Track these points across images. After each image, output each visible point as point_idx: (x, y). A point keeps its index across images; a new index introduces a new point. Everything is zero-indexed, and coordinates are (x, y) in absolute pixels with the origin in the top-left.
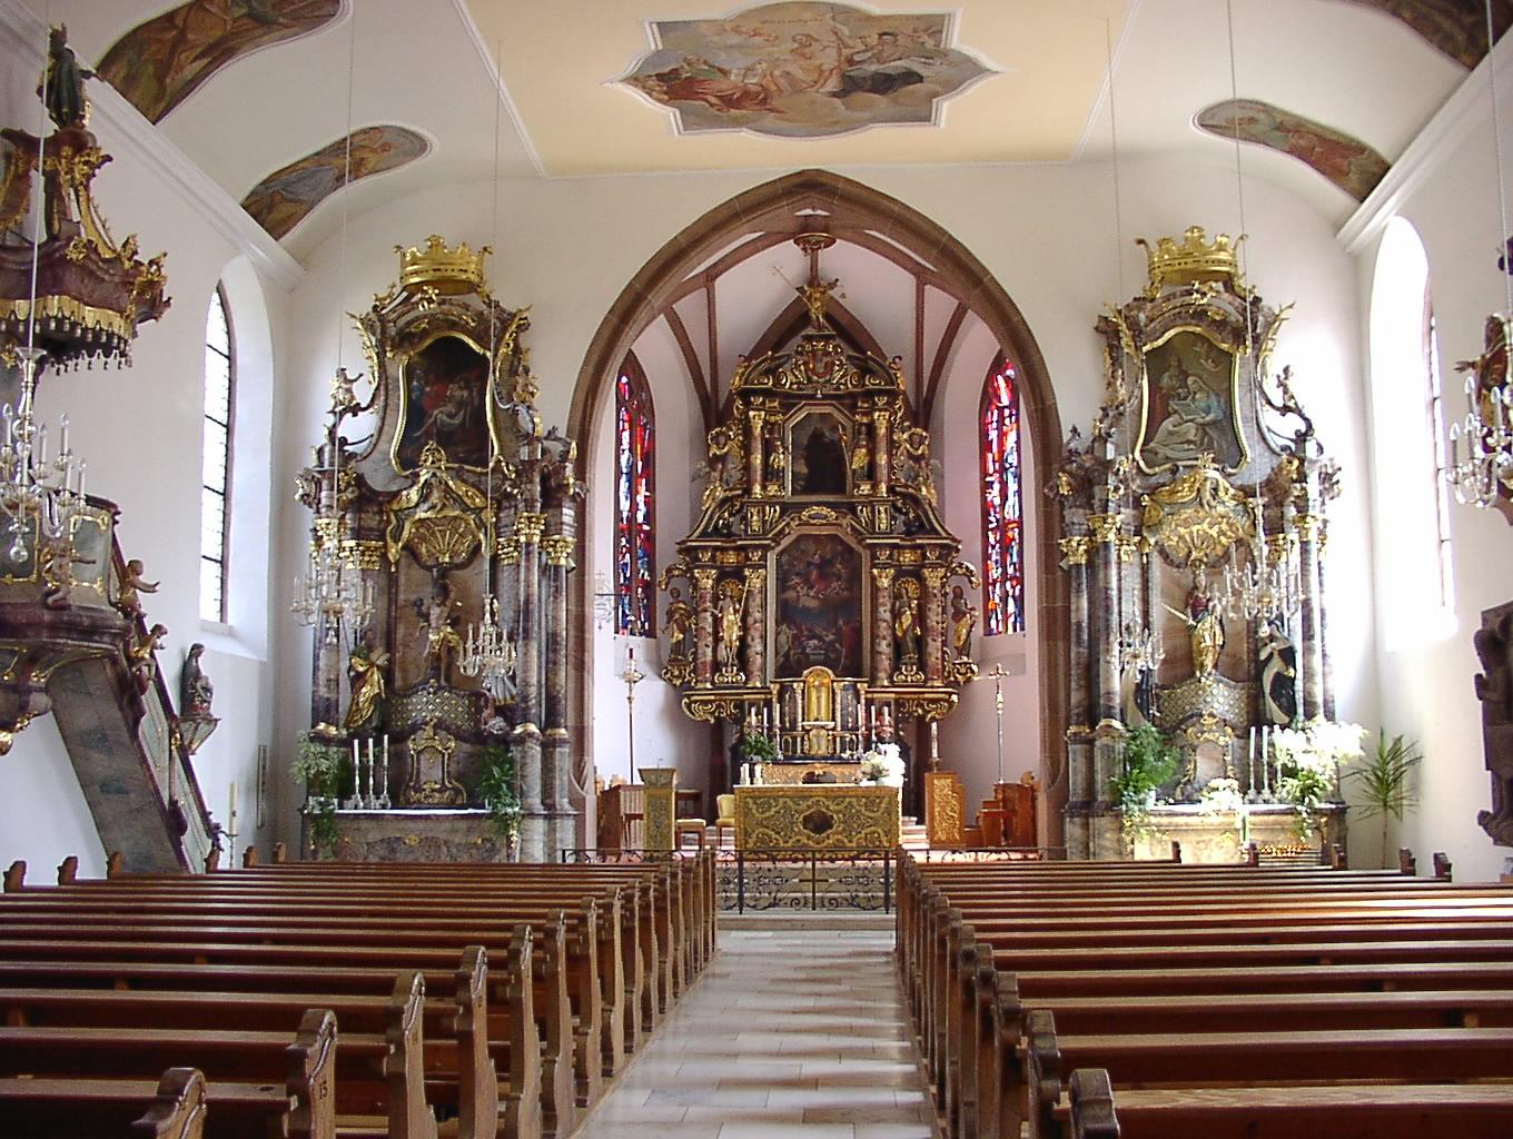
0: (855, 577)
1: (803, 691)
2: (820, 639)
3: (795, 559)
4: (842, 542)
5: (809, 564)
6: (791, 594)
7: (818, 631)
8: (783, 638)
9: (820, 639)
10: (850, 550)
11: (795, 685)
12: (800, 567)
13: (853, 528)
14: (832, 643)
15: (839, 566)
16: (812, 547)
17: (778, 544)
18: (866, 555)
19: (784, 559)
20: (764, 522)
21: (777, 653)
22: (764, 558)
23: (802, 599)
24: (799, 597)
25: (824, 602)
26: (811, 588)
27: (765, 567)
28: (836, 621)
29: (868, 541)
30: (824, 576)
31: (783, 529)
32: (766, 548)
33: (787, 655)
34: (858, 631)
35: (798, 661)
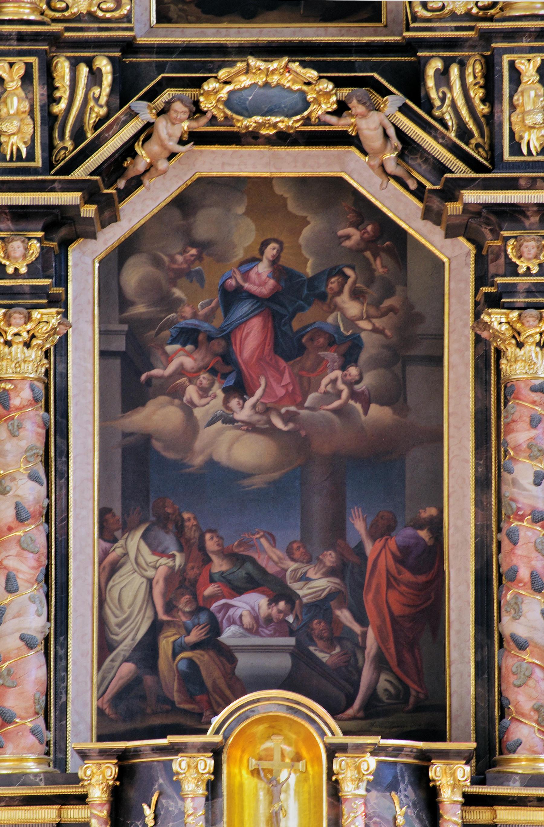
0: (415, 349)
1: (213, 788)
2: (280, 592)
3: (177, 276)
4: (365, 211)
5: (231, 297)
6: (159, 416)
7: (271, 556)
8: (130, 586)
9: (280, 592)
10: (392, 238)
11: (180, 763)
12: (196, 306)
13: (408, 147)
14: (321, 607)
15: (353, 308)
16: (243, 233)
17: (109, 212)
18: (456, 256)
19: (134, 274)
20: (50, 121)
21: (105, 646)
22: (53, 265)
23: (206, 434)
24: (191, 426)
25: (297, 444)
26: (240, 389)
27: (58, 302)
28: (338, 527)
29: (471, 196)
30: (287, 346)
31: (128, 151)
32: (61, 227)
33: (147, 652)
34: (428, 560)
35: (191, 677)
